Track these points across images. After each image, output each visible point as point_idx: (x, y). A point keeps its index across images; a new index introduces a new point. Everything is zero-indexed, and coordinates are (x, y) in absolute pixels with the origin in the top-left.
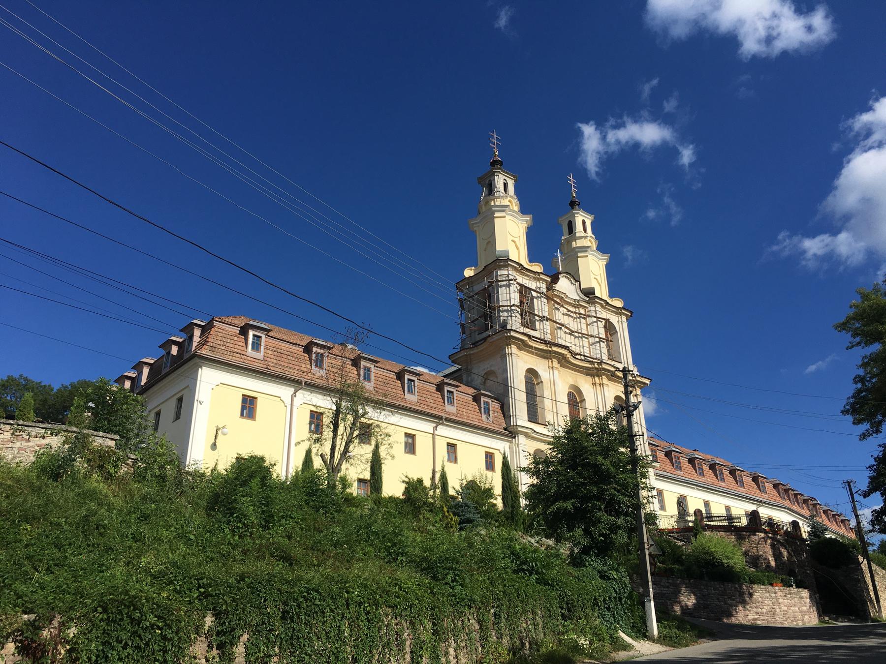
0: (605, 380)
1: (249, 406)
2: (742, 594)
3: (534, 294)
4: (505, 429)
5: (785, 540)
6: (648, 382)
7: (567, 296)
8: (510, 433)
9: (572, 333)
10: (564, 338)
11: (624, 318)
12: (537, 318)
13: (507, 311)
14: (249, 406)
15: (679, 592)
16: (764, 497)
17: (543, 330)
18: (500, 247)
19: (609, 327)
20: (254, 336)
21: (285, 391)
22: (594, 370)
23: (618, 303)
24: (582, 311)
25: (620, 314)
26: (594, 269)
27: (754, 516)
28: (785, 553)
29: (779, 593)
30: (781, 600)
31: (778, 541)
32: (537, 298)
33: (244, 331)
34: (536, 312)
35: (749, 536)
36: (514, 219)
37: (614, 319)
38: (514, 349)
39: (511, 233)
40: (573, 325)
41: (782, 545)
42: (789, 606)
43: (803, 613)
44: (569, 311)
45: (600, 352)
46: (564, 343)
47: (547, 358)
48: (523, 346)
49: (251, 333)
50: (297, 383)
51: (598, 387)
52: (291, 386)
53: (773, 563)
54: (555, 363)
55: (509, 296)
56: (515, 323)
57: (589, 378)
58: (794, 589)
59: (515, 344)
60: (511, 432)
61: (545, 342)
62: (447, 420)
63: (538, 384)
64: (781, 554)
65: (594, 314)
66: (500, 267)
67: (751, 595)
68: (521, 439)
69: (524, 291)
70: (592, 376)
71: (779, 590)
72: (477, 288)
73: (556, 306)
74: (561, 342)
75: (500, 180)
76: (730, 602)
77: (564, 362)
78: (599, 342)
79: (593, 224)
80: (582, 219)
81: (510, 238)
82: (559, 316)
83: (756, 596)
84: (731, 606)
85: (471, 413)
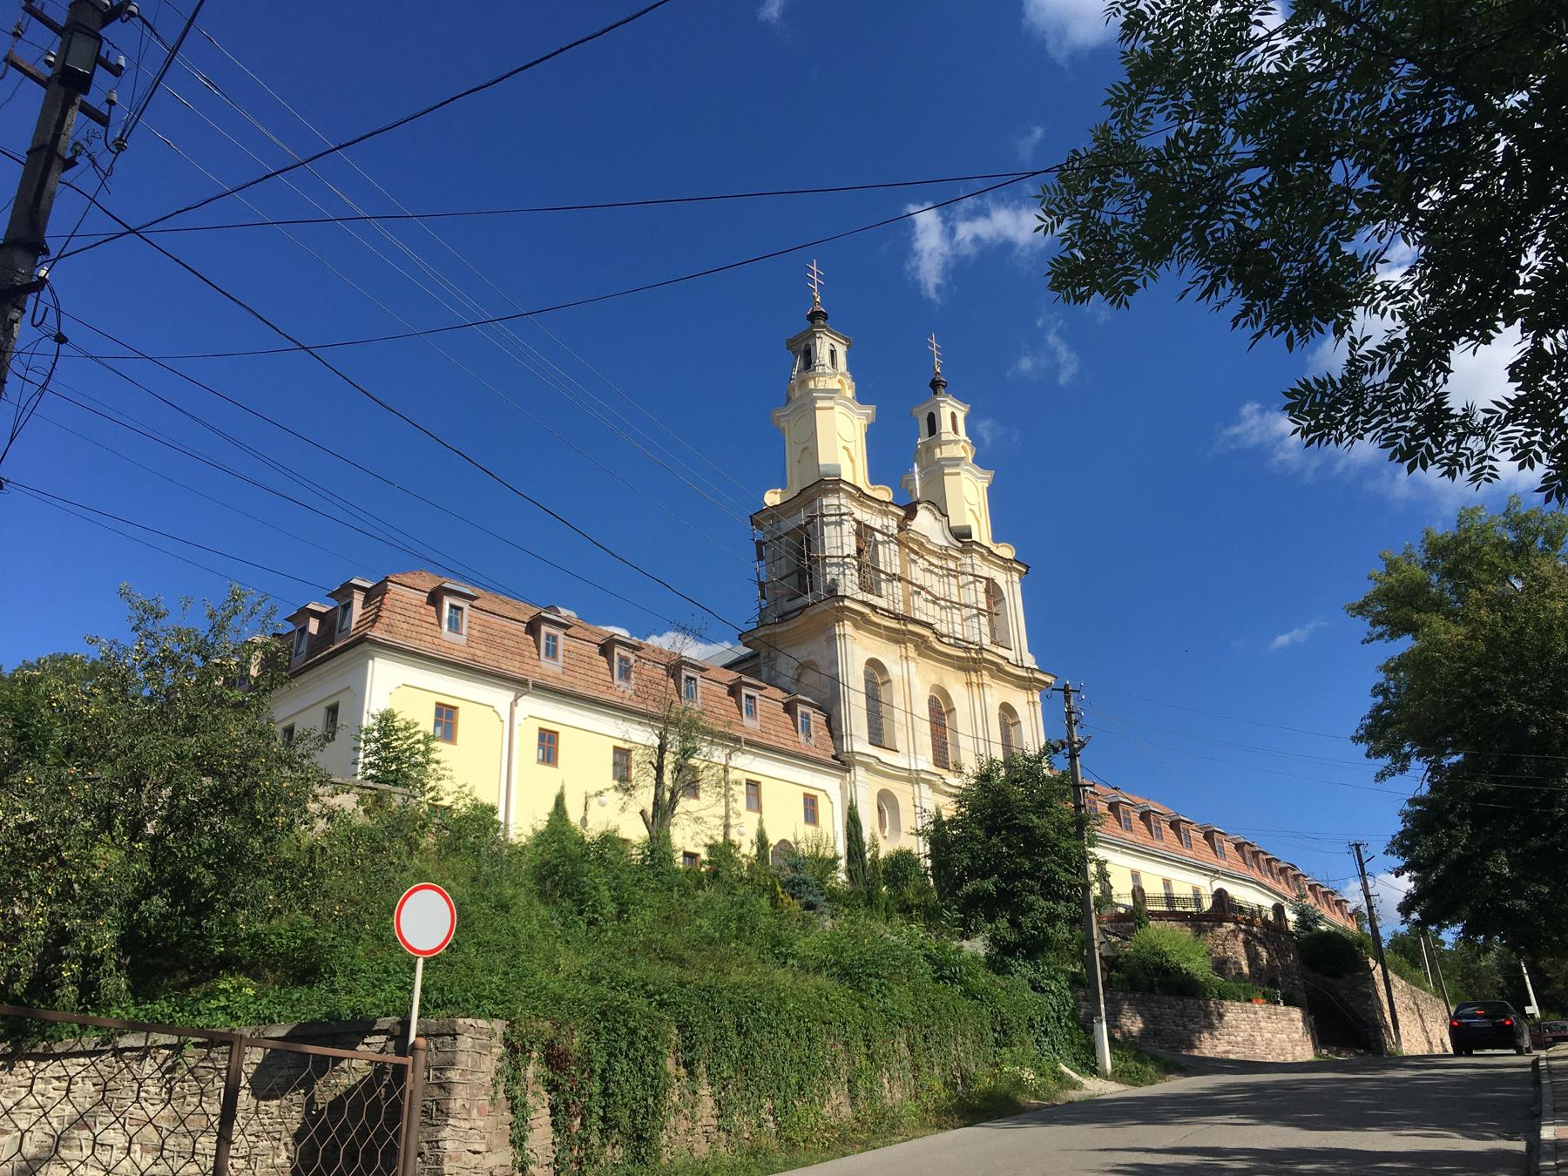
0: (986, 678)
1: (548, 744)
2: (1208, 1015)
3: (879, 537)
4: (834, 757)
5: (1265, 935)
8: (842, 763)
9: (935, 600)
10: (924, 610)
11: (1016, 577)
12: (883, 576)
13: (837, 565)
14: (548, 744)
15: (1120, 1012)
16: (1221, 865)
17: (891, 596)
18: (823, 460)
19: (993, 590)
20: (452, 606)
21: (501, 697)
22: (971, 662)
23: (1007, 552)
24: (952, 565)
25: (1010, 570)
26: (969, 495)
27: (1220, 895)
28: (1264, 954)
29: (1261, 1013)
30: (1263, 1024)
31: (1254, 935)
32: (883, 543)
33: (435, 598)
34: (882, 567)
35: (1212, 929)
36: (846, 411)
37: (1000, 578)
38: (847, 628)
39: (841, 434)
40: (938, 587)
41: (1260, 942)
42: (1274, 1033)
43: (1294, 1043)
44: (931, 564)
45: (978, 631)
46: (924, 618)
48: (863, 623)
49: (447, 602)
50: (519, 684)
51: (975, 688)
52: (509, 688)
53: (1246, 970)
54: (912, 652)
55: (839, 541)
56: (849, 584)
57: (962, 675)
58: (1281, 1008)
59: (849, 618)
60: (843, 763)
61: (897, 617)
62: (749, 743)
63: (884, 683)
64: (1258, 954)
65: (969, 570)
66: (826, 493)
67: (1221, 1016)
68: (860, 772)
69: (863, 531)
71: (1260, 1009)
72: (788, 524)
73: (913, 556)
74: (918, 616)
75: (824, 345)
76: (1191, 1026)
77: (924, 648)
78: (977, 616)
79: (967, 419)
80: (950, 410)
81: (840, 443)
82: (917, 574)
83: (1229, 1017)
84: (1193, 1032)
85: (781, 731)
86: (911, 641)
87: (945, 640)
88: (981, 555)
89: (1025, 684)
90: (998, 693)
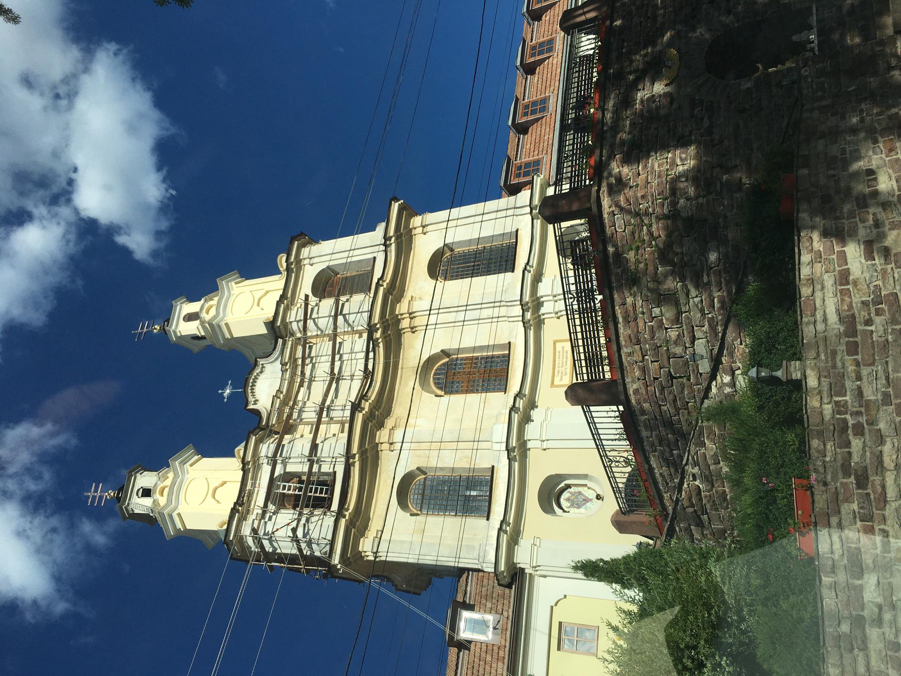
0: (402, 308)
6: (395, 207)
7: (279, 391)
9: (335, 378)
11: (305, 252)
12: (315, 468)
22: (388, 333)
23: (282, 260)
25: (298, 261)
37: (309, 275)
38: (366, 546)
47: (378, 452)
48: (359, 523)
57: (407, 338)
65: (301, 324)
68: (522, 558)
69: (277, 499)
70: (399, 334)
73: (295, 416)
78: (344, 316)
86: (373, 436)
87: (370, 367)
88: (287, 309)
89: (403, 242)
90: (420, 285)
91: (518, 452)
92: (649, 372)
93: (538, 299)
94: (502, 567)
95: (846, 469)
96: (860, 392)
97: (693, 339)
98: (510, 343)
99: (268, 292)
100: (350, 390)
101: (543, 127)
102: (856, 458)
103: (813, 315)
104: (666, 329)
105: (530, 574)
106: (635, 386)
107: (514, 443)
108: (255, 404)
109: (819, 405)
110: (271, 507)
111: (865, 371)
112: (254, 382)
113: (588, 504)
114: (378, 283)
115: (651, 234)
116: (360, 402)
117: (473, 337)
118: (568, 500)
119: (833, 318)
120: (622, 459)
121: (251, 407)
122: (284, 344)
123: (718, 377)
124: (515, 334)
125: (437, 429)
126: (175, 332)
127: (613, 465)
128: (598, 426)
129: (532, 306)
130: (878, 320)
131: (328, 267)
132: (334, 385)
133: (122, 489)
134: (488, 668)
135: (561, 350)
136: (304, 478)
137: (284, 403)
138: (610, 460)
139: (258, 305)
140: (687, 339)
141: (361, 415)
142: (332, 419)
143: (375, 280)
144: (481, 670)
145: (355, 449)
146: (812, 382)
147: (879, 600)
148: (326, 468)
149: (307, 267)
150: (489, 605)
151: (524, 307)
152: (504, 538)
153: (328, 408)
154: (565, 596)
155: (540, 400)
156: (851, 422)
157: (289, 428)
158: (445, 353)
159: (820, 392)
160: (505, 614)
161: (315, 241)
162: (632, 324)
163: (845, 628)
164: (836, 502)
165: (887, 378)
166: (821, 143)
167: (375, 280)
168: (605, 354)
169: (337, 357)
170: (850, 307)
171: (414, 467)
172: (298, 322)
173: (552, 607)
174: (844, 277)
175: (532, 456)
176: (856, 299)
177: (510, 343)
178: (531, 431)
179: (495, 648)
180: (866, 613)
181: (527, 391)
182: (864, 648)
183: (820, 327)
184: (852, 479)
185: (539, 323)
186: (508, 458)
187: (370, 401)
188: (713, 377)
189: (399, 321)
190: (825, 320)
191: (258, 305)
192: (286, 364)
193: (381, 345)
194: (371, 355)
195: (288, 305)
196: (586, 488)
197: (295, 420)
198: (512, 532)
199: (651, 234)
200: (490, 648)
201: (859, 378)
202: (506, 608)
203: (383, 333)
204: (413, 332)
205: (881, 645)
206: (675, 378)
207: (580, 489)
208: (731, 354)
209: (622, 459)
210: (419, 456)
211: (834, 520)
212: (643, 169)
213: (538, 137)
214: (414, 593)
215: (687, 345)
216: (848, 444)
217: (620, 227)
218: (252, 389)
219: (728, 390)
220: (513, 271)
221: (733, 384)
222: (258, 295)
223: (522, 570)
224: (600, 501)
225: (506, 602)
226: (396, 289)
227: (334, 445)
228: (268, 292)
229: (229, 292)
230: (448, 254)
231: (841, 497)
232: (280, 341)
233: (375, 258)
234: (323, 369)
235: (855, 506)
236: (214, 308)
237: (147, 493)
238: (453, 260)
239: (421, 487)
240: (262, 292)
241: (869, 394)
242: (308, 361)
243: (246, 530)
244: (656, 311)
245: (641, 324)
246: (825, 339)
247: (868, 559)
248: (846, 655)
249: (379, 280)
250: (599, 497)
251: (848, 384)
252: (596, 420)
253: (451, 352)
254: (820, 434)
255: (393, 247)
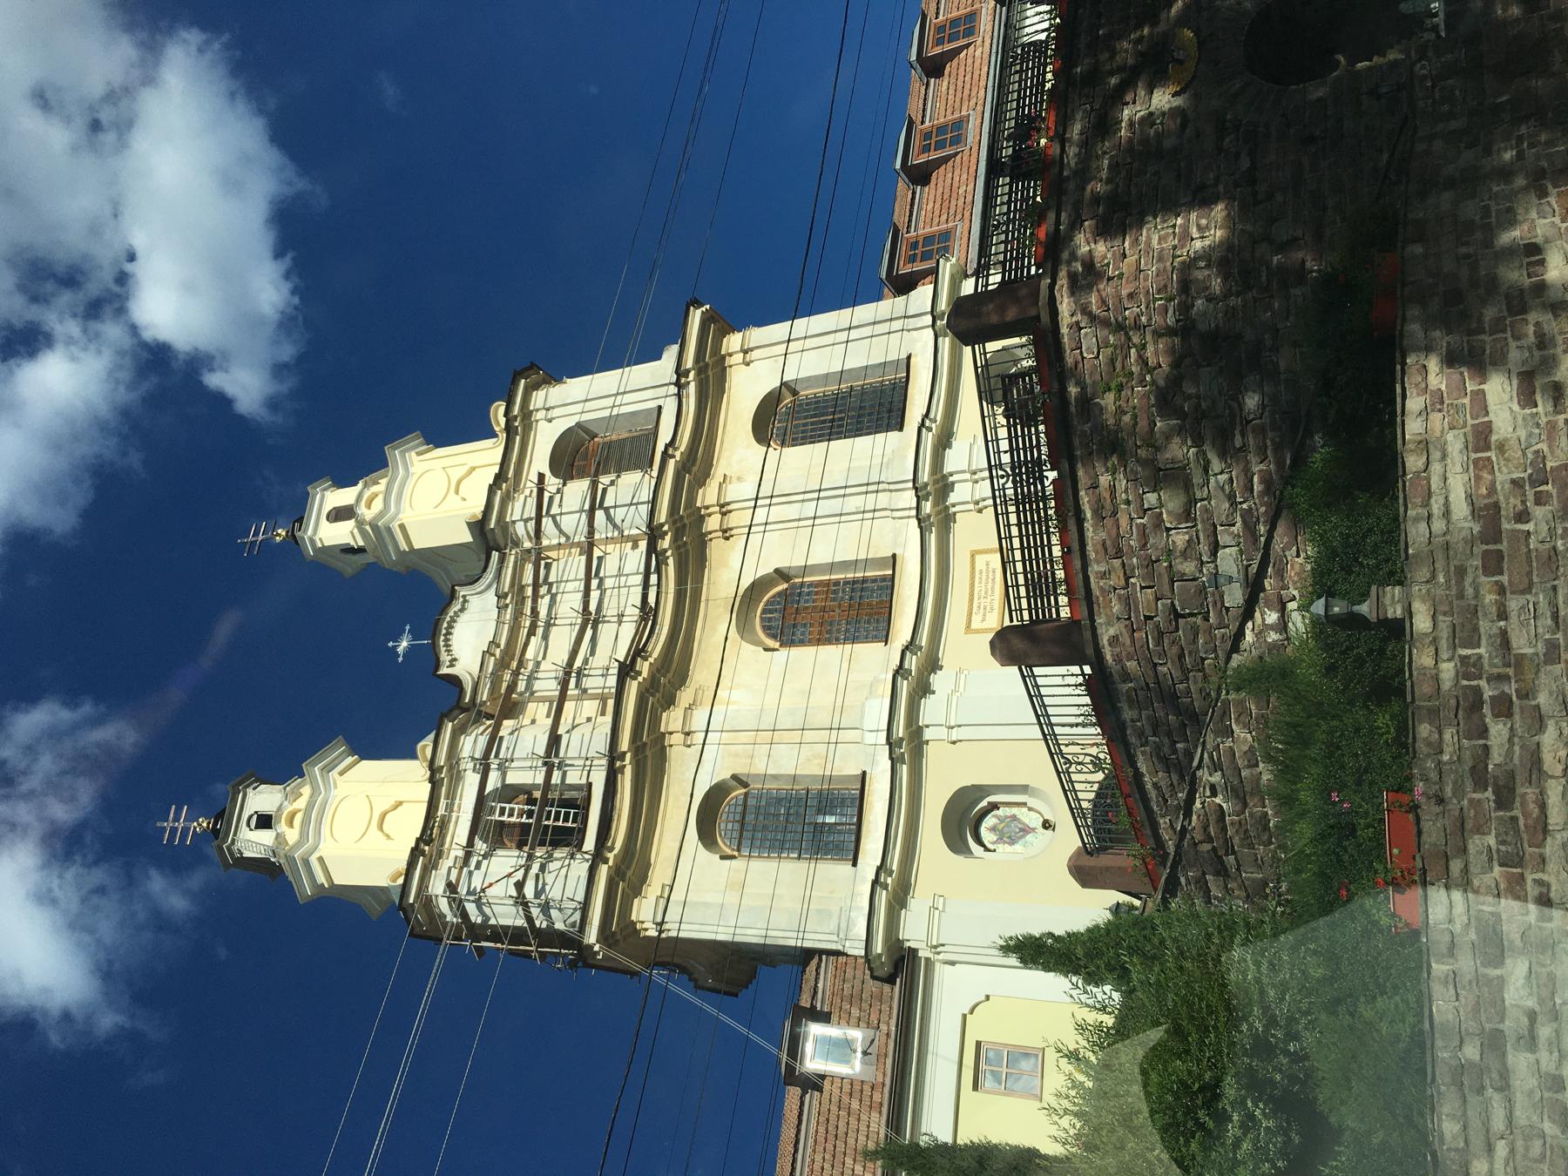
0: (708, 496)
6: (696, 317)
7: (494, 643)
9: (591, 619)
11: (538, 398)
12: (556, 778)
22: (682, 541)
23: (498, 412)
25: (527, 414)
38: (644, 912)
44: (532, 632)
47: (663, 748)
48: (630, 873)
57: (716, 548)
68: (913, 931)
69: (490, 831)
70: (702, 542)
73: (521, 686)
78: (607, 510)
86: (656, 721)
88: (507, 499)
89: (710, 379)
90: (739, 456)
91: (908, 747)
92: (1137, 607)
93: (945, 477)
94: (878, 947)
95: (1479, 776)
96: (1504, 640)
97: (1215, 548)
98: (894, 556)
99: (473, 469)
100: (615, 641)
101: (957, 172)
102: (1496, 757)
103: (1426, 504)
104: (1168, 530)
105: (927, 959)
106: (1112, 632)
107: (900, 730)
108: (452, 665)
109: (1434, 665)
110: (481, 846)
111: (1514, 604)
112: (450, 627)
113: (1029, 837)
114: (665, 453)
115: (1143, 361)
116: (634, 661)
117: (830, 548)
118: (993, 829)
119: (1460, 509)
120: (1088, 759)
121: (444, 670)
122: (502, 560)
123: (1257, 615)
124: (904, 540)
125: (764, 708)
126: (312, 541)
127: (1073, 769)
128: (1047, 701)
129: (934, 491)
130: (1539, 512)
131: (578, 425)
132: (589, 632)
133: (222, 815)
134: (853, 1121)
135: (984, 568)
136: (537, 794)
137: (502, 664)
138: (1068, 761)
139: (457, 492)
140: (1204, 548)
141: (635, 684)
142: (585, 691)
143: (660, 448)
144: (842, 1125)
145: (624, 745)
146: (1422, 623)
147: (1531, 1003)
148: (574, 777)
149: (542, 425)
150: (855, 1012)
151: (920, 492)
152: (883, 898)
153: (579, 673)
154: (988, 998)
155: (947, 655)
156: (1488, 692)
157: (511, 708)
158: (782, 575)
159: (1435, 641)
160: (884, 1027)
161: (554, 378)
162: (1109, 522)
163: (1471, 1052)
164: (1461, 829)
165: (1555, 616)
166: (1446, 198)
167: (660, 448)
168: (1060, 574)
169: (595, 583)
170: (1492, 490)
171: (726, 775)
172: (526, 521)
173: (964, 1016)
174: (1482, 437)
175: (931, 752)
176: (1502, 477)
177: (894, 556)
178: (931, 710)
179: (867, 1088)
180: (1507, 1026)
181: (924, 639)
182: (1504, 1087)
183: (1438, 525)
184: (1489, 794)
185: (946, 520)
186: (891, 758)
187: (651, 660)
188: (1248, 613)
189: (702, 519)
190: (1447, 513)
191: (457, 492)
192: (505, 596)
193: (671, 561)
194: (654, 579)
195: (508, 492)
196: (1025, 810)
197: (521, 694)
198: (895, 887)
199: (1143, 361)
200: (857, 1087)
201: (1503, 615)
202: (884, 1017)
203: (675, 540)
204: (727, 539)
205: (1533, 1082)
206: (1183, 616)
207: (1015, 811)
208: (1280, 574)
209: (1088, 759)
210: (736, 755)
211: (1456, 866)
212: (1132, 245)
213: (947, 190)
214: (726, 993)
215: (1205, 559)
216: (1484, 732)
217: (1089, 350)
218: (447, 640)
219: (1273, 637)
220: (901, 429)
221: (1282, 626)
222: (456, 474)
223: (913, 952)
224: (1049, 832)
225: (885, 1007)
226: (697, 463)
227: (589, 735)
228: (473, 469)
229: (407, 470)
230: (788, 400)
231: (1469, 825)
232: (495, 555)
233: (660, 407)
234: (570, 604)
235: (1491, 840)
236: (380, 499)
237: (265, 821)
238: (797, 409)
239: (739, 809)
240: (463, 471)
241: (1521, 644)
242: (543, 590)
243: (437, 886)
244: (1151, 498)
245: (1124, 521)
246: (1447, 546)
247: (1512, 931)
248: (1473, 1100)
249: (667, 446)
250: (1047, 825)
251: (1484, 625)
252: (1043, 691)
253: (792, 573)
254: (1434, 714)
255: (692, 388)
